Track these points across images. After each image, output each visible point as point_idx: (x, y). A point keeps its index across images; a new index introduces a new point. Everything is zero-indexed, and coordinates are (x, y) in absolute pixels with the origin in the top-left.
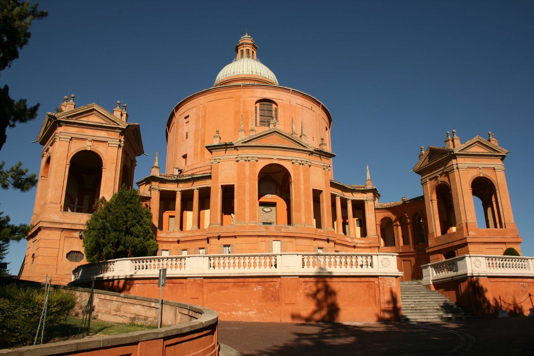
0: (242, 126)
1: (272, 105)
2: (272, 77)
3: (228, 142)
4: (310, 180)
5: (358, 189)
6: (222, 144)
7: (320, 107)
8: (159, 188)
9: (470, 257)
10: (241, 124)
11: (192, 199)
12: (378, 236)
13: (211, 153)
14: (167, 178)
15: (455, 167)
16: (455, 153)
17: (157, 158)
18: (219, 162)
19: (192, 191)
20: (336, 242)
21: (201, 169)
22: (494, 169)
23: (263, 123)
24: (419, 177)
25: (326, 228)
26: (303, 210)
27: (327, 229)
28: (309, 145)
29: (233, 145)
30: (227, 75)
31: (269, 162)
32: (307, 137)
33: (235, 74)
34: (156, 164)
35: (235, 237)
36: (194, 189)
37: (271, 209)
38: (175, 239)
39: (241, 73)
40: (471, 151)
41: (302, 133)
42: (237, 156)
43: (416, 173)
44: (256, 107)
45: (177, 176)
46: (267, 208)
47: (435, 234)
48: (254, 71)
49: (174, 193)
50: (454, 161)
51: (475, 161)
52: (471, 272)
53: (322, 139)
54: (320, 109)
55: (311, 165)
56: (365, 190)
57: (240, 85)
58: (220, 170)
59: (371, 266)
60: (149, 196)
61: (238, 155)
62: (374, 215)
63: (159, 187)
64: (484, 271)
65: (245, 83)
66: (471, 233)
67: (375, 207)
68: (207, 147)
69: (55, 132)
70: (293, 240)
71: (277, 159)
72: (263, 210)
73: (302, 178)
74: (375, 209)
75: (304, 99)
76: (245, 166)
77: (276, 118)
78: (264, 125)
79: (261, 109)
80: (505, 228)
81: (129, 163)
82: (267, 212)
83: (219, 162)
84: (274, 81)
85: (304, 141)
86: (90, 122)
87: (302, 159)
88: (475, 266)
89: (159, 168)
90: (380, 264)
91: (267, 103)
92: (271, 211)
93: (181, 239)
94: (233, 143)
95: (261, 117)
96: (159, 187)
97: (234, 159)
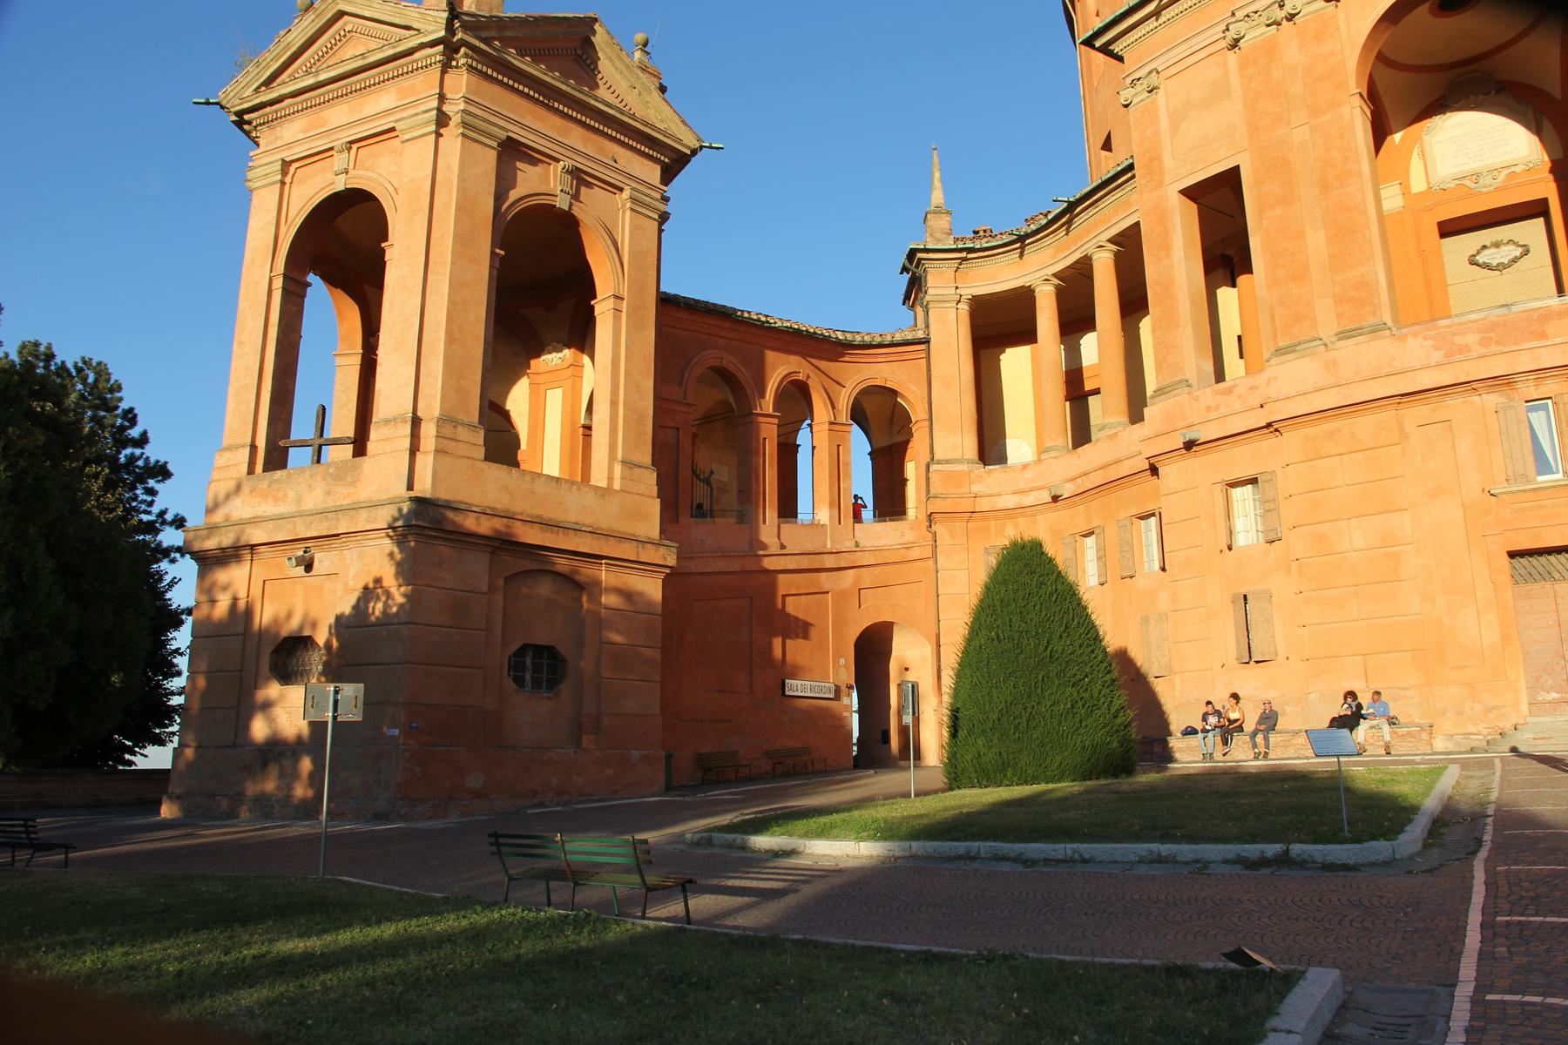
13: (1120, 59)
17: (937, 174)
34: (937, 197)
37: (1525, 246)
42: (1233, 20)
46: (1497, 245)
49: (1023, 299)
58: (1164, 123)
60: (920, 334)
61: (1233, 14)
63: (957, 288)
72: (1473, 262)
76: (1270, 50)
82: (1500, 267)
89: (948, 213)
92: (1526, 252)
96: (957, 288)
97: (1223, 44)
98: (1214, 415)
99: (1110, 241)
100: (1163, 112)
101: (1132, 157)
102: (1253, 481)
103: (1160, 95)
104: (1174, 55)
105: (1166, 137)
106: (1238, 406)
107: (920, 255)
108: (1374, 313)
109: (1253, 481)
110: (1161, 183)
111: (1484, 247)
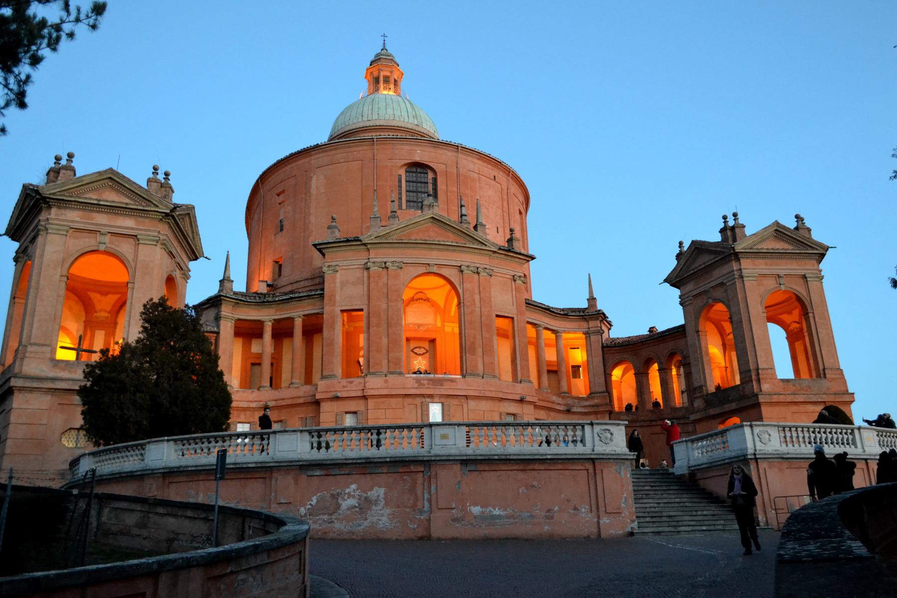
0: (376, 209)
1: (427, 173)
2: (428, 123)
3: (351, 236)
4: (493, 299)
5: (574, 314)
6: (342, 240)
7: (508, 175)
8: (233, 315)
10: (374, 206)
11: (290, 334)
12: (609, 393)
13: (324, 255)
14: (248, 298)
15: (737, 274)
16: (737, 251)
18: (337, 271)
19: (291, 320)
20: (536, 404)
21: (307, 283)
22: (804, 277)
23: (412, 204)
24: (677, 292)
25: (519, 380)
26: (479, 351)
27: (521, 382)
28: (489, 240)
29: (360, 241)
30: (352, 120)
32: (487, 227)
33: (365, 119)
35: (365, 397)
36: (295, 317)
38: (261, 403)
39: (375, 117)
40: (765, 248)
41: (477, 221)
42: (367, 261)
43: (671, 285)
44: (400, 176)
45: (265, 295)
46: (420, 348)
47: (704, 388)
48: (397, 113)
49: (260, 324)
50: (735, 266)
51: (771, 265)
53: (512, 230)
54: (511, 180)
55: (494, 274)
56: (586, 315)
57: (373, 138)
58: (338, 285)
59: (581, 441)
60: (215, 329)
62: (601, 358)
64: (776, 450)
65: (380, 135)
66: (765, 387)
67: (602, 344)
68: (315, 245)
69: (41, 218)
70: (463, 400)
71: (436, 264)
72: (413, 352)
73: (477, 297)
74: (603, 347)
75: (480, 162)
77: (435, 196)
78: (413, 207)
79: (408, 179)
80: (825, 377)
81: (177, 274)
83: (337, 271)
84: (431, 131)
85: (479, 234)
86: (104, 201)
87: (478, 265)
88: (761, 441)
90: (597, 438)
91: (419, 170)
93: (271, 404)
94: (361, 238)
95: (408, 193)
98: (345, 389)
99: (304, 315)
100: (338, 280)
101: (323, 289)
102: (355, 413)
103: (338, 275)
104: (345, 263)
105: (338, 290)
106: (354, 388)
107: (222, 298)
108: (400, 368)
109: (355, 413)
110: (334, 305)
111: (416, 347)
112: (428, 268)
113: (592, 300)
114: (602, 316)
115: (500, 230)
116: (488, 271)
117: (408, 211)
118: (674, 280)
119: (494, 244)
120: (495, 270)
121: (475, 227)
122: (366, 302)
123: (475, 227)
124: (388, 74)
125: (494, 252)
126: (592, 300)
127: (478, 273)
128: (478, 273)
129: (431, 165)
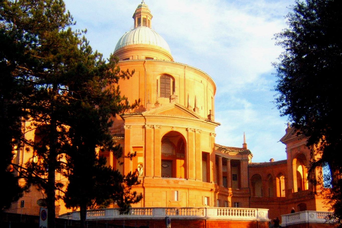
9: (308, 212)
24: (284, 146)
26: (194, 168)
31: (170, 130)
44: (157, 80)
52: (308, 220)
53: (210, 111)
76: (150, 131)
82: (165, 168)
85: (196, 113)
112: (172, 128)
113: (245, 144)
114: (248, 152)
115: (203, 108)
116: (199, 131)
117: (161, 98)
118: (284, 140)
119: (202, 118)
120: (203, 130)
121: (194, 110)
122: (144, 143)
123: (194, 110)
124: (145, 17)
125: (203, 122)
126: (245, 144)
127: (195, 132)
128: (195, 132)
129: (173, 75)
